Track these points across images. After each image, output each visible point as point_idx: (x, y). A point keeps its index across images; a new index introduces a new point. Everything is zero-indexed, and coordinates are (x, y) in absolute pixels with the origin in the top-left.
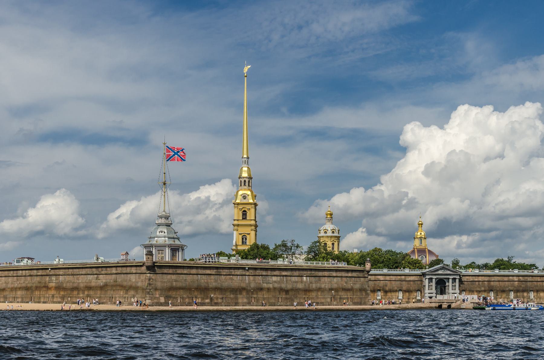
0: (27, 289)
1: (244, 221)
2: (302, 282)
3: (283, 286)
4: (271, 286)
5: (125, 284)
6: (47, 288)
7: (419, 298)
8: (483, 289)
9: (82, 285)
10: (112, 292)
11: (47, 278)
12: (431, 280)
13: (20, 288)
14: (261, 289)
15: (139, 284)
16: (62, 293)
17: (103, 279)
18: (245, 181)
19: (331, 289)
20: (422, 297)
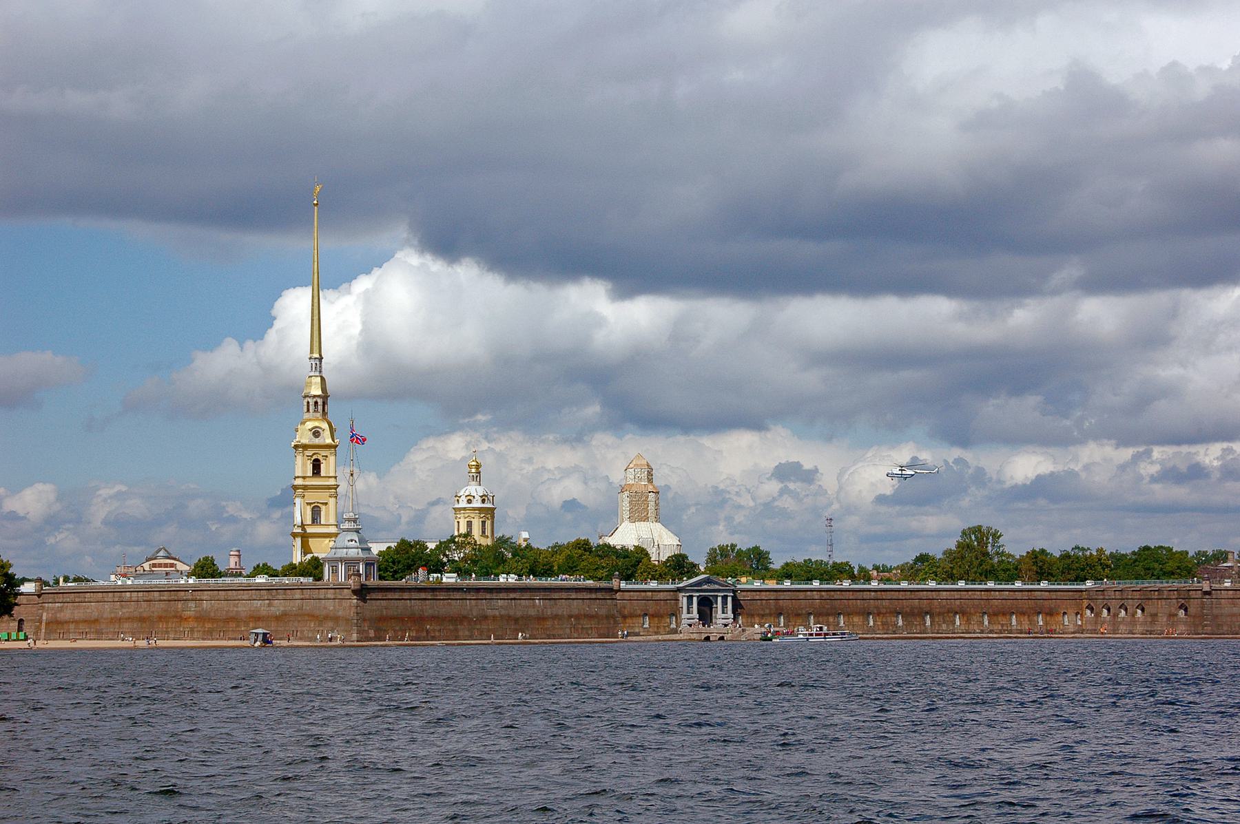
0: (142, 620)
2: (534, 606)
3: (512, 613)
4: (497, 613)
5: (317, 613)
6: (181, 619)
7: (673, 626)
8: (767, 611)
10: (296, 624)
11: (180, 605)
12: (690, 598)
14: (486, 617)
19: (570, 616)
20: (678, 625)
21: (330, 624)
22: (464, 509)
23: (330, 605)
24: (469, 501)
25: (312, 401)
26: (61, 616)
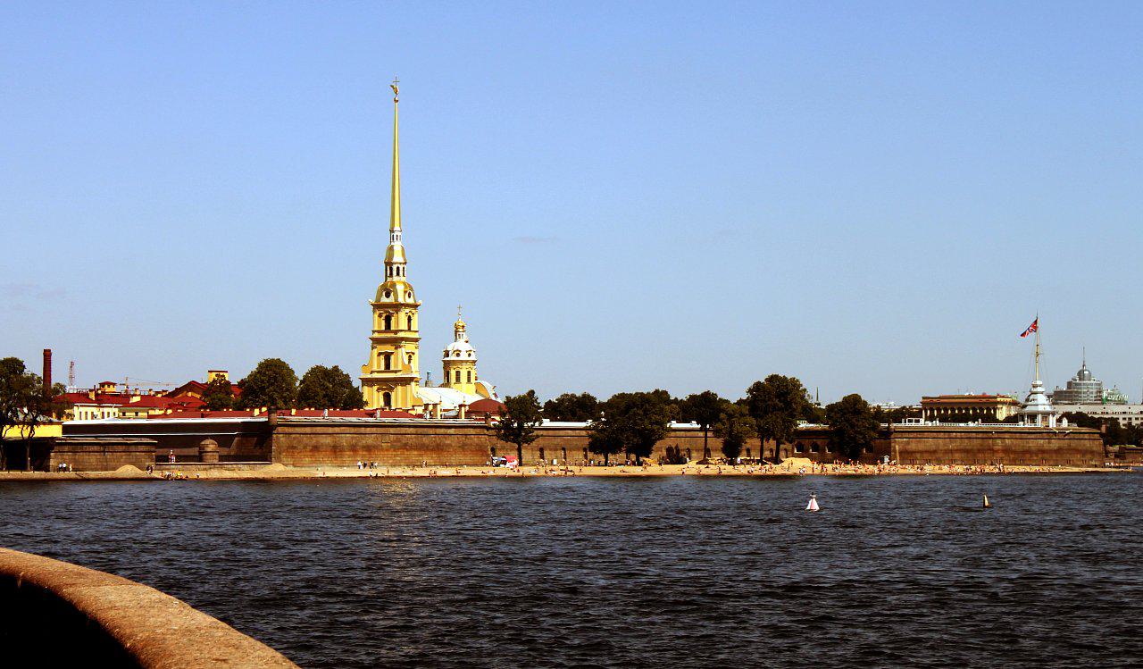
0: (967, 451)
9: (1033, 448)
11: (991, 441)
13: (957, 451)
15: (1094, 449)
17: (1055, 444)
21: (1089, 456)
22: (467, 362)
26: (909, 447)
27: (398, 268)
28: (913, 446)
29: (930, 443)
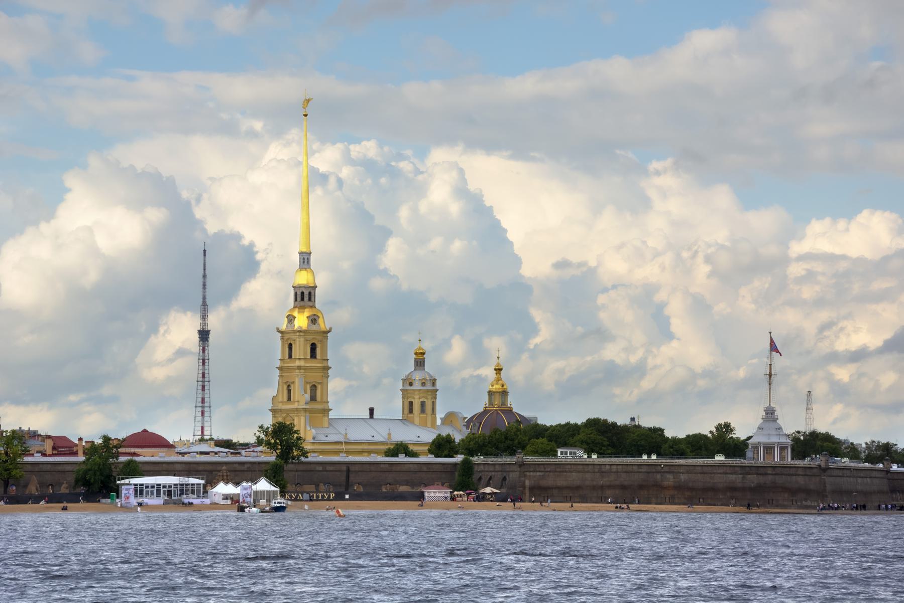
0: (623, 487)
1: (313, 360)
11: (659, 476)
13: (610, 487)
15: (812, 487)
16: (687, 494)
18: (310, 293)
23: (801, 480)
24: (423, 384)
25: (306, 293)
26: (544, 483)
27: (303, 293)
28: (549, 481)
29: (574, 478)
